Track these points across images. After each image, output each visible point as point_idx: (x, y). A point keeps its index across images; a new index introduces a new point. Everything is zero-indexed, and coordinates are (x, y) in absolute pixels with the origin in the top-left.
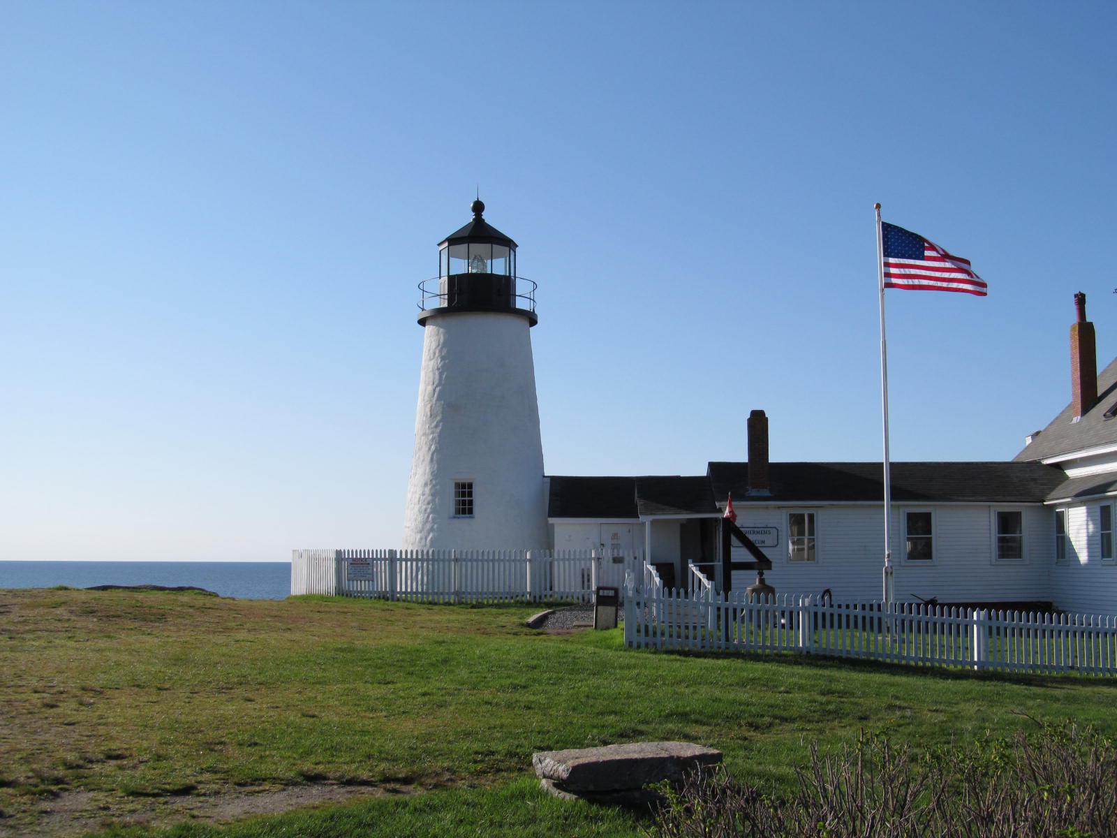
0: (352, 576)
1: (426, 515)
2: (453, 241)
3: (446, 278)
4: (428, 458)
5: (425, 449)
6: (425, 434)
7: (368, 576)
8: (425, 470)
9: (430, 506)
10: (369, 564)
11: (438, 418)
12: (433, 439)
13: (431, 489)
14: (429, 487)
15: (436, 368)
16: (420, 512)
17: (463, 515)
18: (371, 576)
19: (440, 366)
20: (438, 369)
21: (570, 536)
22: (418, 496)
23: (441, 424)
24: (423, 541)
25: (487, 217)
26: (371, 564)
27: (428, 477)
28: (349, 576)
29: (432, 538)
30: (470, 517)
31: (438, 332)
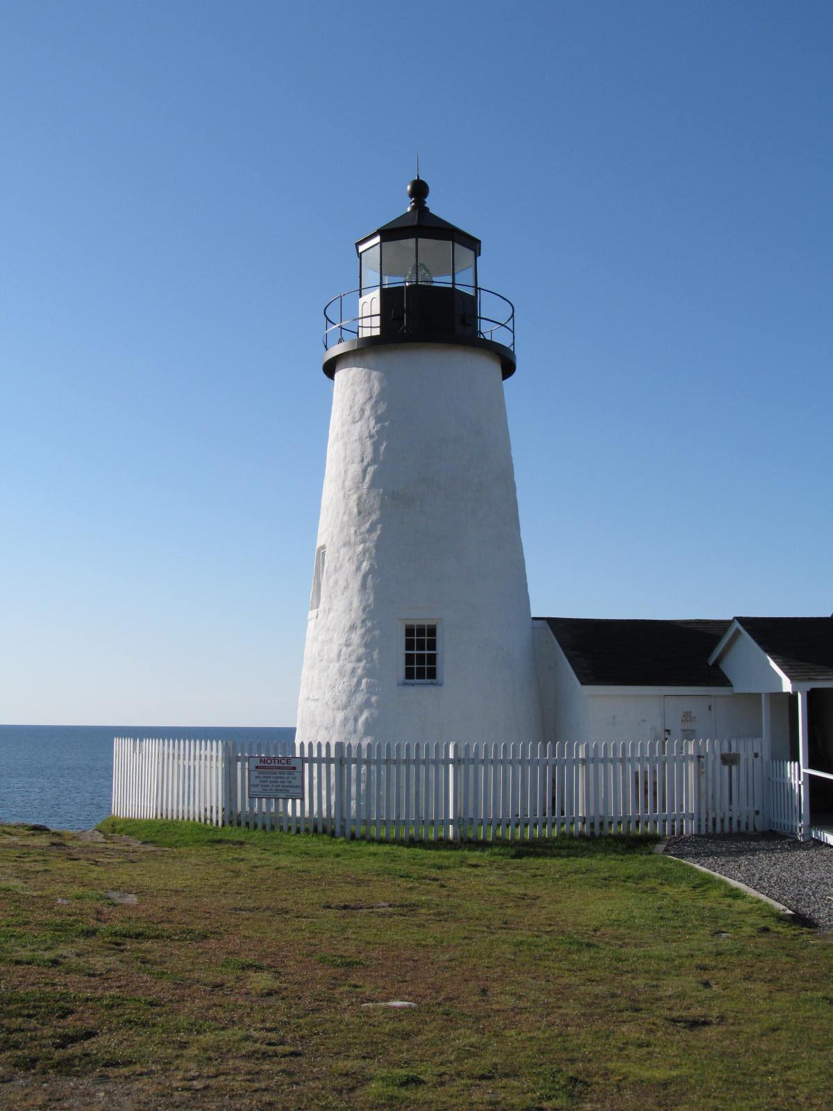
0: (260, 789)
1: (355, 680)
2: (389, 234)
3: (376, 293)
4: (356, 584)
5: (349, 567)
6: (347, 544)
7: (291, 790)
8: (351, 604)
9: (362, 664)
10: (294, 768)
11: (374, 517)
12: (364, 552)
13: (363, 636)
14: (360, 632)
15: (366, 434)
16: (341, 672)
17: (421, 681)
18: (299, 790)
19: (373, 431)
20: (371, 436)
21: (614, 718)
22: (335, 648)
23: (379, 526)
24: (351, 723)
25: (434, 204)
26: (299, 769)
27: (356, 615)
28: (253, 789)
29: (367, 719)
30: (432, 684)
31: (369, 377)
